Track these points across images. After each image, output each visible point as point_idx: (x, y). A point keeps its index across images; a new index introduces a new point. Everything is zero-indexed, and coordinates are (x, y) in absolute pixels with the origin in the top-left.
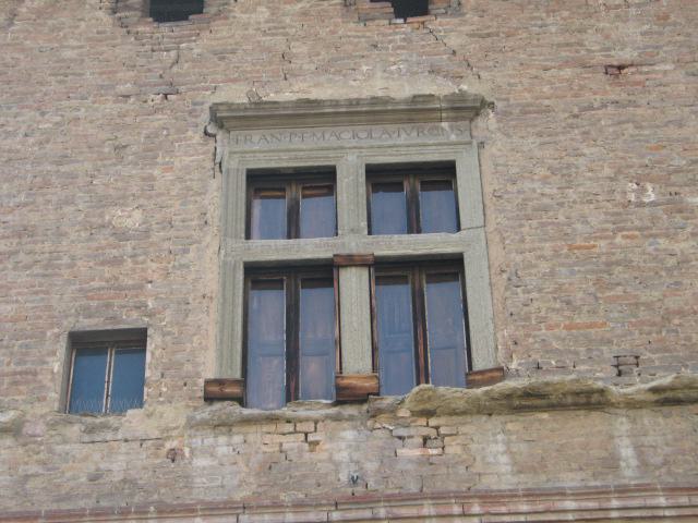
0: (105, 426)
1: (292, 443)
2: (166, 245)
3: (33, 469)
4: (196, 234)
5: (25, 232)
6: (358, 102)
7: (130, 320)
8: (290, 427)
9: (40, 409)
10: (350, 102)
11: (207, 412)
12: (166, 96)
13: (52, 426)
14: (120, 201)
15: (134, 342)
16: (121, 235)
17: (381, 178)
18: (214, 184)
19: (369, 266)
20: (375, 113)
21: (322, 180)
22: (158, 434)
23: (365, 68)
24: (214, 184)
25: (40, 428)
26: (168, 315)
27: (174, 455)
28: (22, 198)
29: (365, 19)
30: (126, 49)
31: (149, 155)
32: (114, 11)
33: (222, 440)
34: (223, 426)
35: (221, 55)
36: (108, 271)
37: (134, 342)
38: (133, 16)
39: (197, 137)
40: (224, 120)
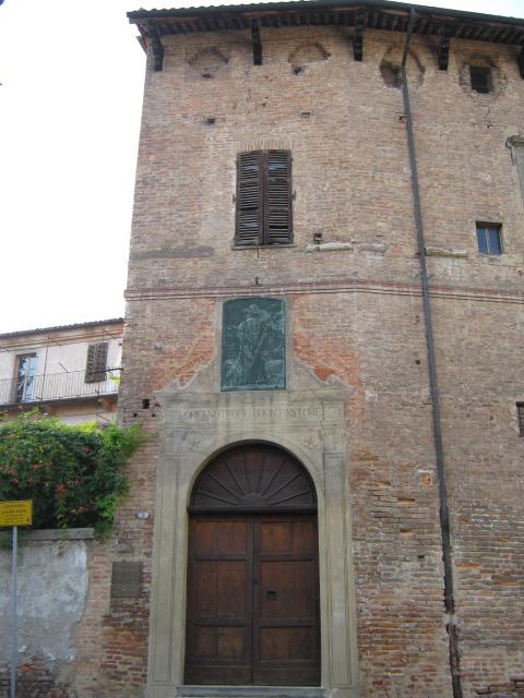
0: (495, 260)
2: (502, 191)
3: (476, 272)
4: (511, 188)
5: (450, 177)
7: (496, 220)
9: (472, 250)
13: (478, 257)
14: (482, 169)
15: (497, 227)
16: (486, 184)
25: (474, 258)
26: (509, 220)
28: (446, 163)
30: (468, 103)
31: (487, 152)
32: (461, 84)
35: (506, 112)
36: (484, 198)
37: (497, 227)
38: (469, 88)
39: (504, 147)
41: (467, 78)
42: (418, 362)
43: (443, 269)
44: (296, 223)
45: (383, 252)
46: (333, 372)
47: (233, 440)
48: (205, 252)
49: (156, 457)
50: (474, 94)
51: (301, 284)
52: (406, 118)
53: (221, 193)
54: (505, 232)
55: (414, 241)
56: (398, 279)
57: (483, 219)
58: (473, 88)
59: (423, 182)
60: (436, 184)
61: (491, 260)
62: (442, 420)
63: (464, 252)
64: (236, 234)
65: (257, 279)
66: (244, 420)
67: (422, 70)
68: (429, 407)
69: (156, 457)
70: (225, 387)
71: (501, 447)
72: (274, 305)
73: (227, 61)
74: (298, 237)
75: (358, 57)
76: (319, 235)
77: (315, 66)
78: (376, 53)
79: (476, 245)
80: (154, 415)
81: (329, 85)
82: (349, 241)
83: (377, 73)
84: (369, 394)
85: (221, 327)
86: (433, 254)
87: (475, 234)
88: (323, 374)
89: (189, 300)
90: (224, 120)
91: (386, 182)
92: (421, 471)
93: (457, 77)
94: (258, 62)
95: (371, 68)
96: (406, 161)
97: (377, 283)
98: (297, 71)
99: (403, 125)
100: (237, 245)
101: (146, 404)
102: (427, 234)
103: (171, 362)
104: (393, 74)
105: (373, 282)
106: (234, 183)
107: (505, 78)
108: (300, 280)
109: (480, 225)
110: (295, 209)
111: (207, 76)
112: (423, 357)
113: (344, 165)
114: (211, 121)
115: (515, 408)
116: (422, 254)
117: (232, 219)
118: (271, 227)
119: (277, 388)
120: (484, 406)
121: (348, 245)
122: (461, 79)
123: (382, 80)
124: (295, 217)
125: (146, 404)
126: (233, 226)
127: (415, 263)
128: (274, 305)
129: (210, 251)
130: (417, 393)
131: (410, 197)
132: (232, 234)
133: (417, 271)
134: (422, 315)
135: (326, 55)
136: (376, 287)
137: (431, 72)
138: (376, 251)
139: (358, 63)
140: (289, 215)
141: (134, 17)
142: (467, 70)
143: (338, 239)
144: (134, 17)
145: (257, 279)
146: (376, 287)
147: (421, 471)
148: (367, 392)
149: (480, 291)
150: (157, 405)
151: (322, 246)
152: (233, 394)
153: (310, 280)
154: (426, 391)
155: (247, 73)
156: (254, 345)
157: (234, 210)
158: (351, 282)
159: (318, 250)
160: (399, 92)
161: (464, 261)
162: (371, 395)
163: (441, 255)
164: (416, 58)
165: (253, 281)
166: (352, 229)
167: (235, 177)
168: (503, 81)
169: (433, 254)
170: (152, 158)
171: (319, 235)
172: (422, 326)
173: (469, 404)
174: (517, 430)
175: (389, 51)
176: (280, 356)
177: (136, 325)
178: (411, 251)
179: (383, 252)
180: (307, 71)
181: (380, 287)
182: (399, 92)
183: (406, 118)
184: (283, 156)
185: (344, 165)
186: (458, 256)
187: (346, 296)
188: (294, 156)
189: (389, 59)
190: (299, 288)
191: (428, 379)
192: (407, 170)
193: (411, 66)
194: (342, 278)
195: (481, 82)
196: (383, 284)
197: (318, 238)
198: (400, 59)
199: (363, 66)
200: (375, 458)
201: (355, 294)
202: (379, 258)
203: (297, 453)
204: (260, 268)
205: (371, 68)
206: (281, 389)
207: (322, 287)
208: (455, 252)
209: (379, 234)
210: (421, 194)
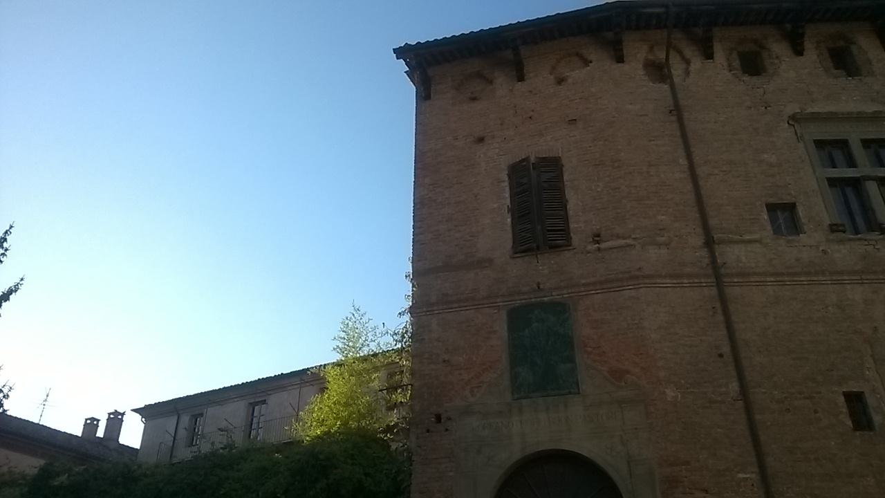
1: (870, 248)
6: (852, 113)
7: (787, 199)
8: (866, 243)
10: (848, 114)
11: (833, 236)
12: (766, 108)
15: (791, 208)
17: (867, 143)
18: (801, 145)
19: (876, 181)
20: (859, 118)
21: (843, 144)
22: (811, 243)
23: (844, 98)
24: (801, 145)
27: (824, 252)
29: (836, 77)
33: (842, 247)
34: (841, 241)
37: (791, 208)
40: (794, 119)
41: (736, 64)
42: (721, 356)
43: (733, 255)
44: (572, 226)
45: (667, 245)
46: (628, 372)
47: (529, 451)
48: (484, 263)
49: (451, 474)
50: (746, 78)
51: (584, 285)
52: (677, 111)
53: (495, 206)
54: (801, 211)
55: (699, 230)
56: (688, 270)
57: (772, 200)
58: (745, 72)
59: (701, 171)
60: (716, 171)
61: (788, 241)
62: (758, 417)
63: (756, 236)
64: (514, 243)
65: (538, 284)
66: (537, 428)
67: (688, 62)
68: (741, 403)
69: (451, 474)
70: (516, 396)
71: (833, 443)
72: (560, 309)
73: (491, 82)
74: (576, 239)
75: (620, 59)
76: (598, 236)
77: (577, 74)
78: (638, 51)
79: (769, 227)
80: (447, 430)
81: (593, 90)
82: (629, 237)
83: (641, 72)
84: (670, 393)
85: (506, 334)
86: (722, 242)
87: (766, 217)
88: (618, 375)
89: (472, 311)
90: (493, 137)
91: (662, 176)
92: (741, 476)
93: (725, 64)
94: (521, 78)
95: (634, 67)
96: (681, 152)
97: (665, 277)
98: (561, 81)
99: (674, 118)
100: (516, 253)
101: (438, 418)
102: (713, 222)
103: (460, 374)
104: (658, 71)
105: (660, 276)
106: (507, 195)
107: (777, 57)
108: (583, 281)
109: (772, 208)
110: (571, 213)
111: (474, 99)
112: (726, 349)
113: (616, 164)
114: (481, 140)
115: (842, 399)
116: (709, 243)
117: (509, 229)
118: (549, 231)
119: (570, 393)
120: (805, 398)
121: (629, 241)
122: (730, 66)
123: (647, 78)
124: (571, 220)
125: (438, 418)
126: (510, 235)
127: (704, 253)
128: (560, 309)
129: (490, 261)
130: (724, 389)
131: (690, 187)
132: (509, 244)
133: (707, 261)
134: (718, 305)
135: (587, 62)
136: (664, 281)
137: (697, 63)
138: (659, 245)
139: (620, 65)
140: (566, 219)
141: (400, 52)
142: (735, 55)
143: (618, 237)
144: (400, 52)
145: (538, 284)
146: (664, 281)
147: (741, 476)
148: (667, 391)
149: (782, 274)
150: (449, 419)
151: (603, 246)
152: (524, 402)
153: (593, 280)
154: (734, 386)
155: (511, 90)
156: (542, 350)
157: (509, 220)
158: (637, 277)
159: (599, 249)
160: (666, 87)
161: (758, 245)
162: (673, 394)
163: (732, 242)
164: (680, 52)
165: (535, 286)
166: (632, 226)
167: (507, 189)
168: (776, 61)
169: (722, 242)
170: (427, 180)
171: (598, 236)
172: (720, 318)
173: (786, 398)
174: (849, 423)
175: (651, 49)
176: (571, 360)
177: (423, 339)
178: (697, 240)
179: (667, 245)
180: (570, 80)
181: (668, 281)
182: (666, 87)
183: (677, 111)
184: (553, 165)
185: (616, 164)
186: (750, 242)
187: (633, 293)
188: (564, 161)
189: (651, 57)
190: (582, 289)
191: (734, 373)
192: (683, 161)
193: (675, 61)
194: (627, 275)
195: (752, 65)
196: (671, 276)
197: (597, 238)
198: (662, 56)
199: (625, 67)
200: (688, 463)
201: (642, 290)
202: (664, 251)
203: (600, 462)
204: (543, 271)
205: (634, 67)
206: (575, 394)
207: (605, 286)
208: (747, 237)
209: (661, 227)
210: (701, 183)
